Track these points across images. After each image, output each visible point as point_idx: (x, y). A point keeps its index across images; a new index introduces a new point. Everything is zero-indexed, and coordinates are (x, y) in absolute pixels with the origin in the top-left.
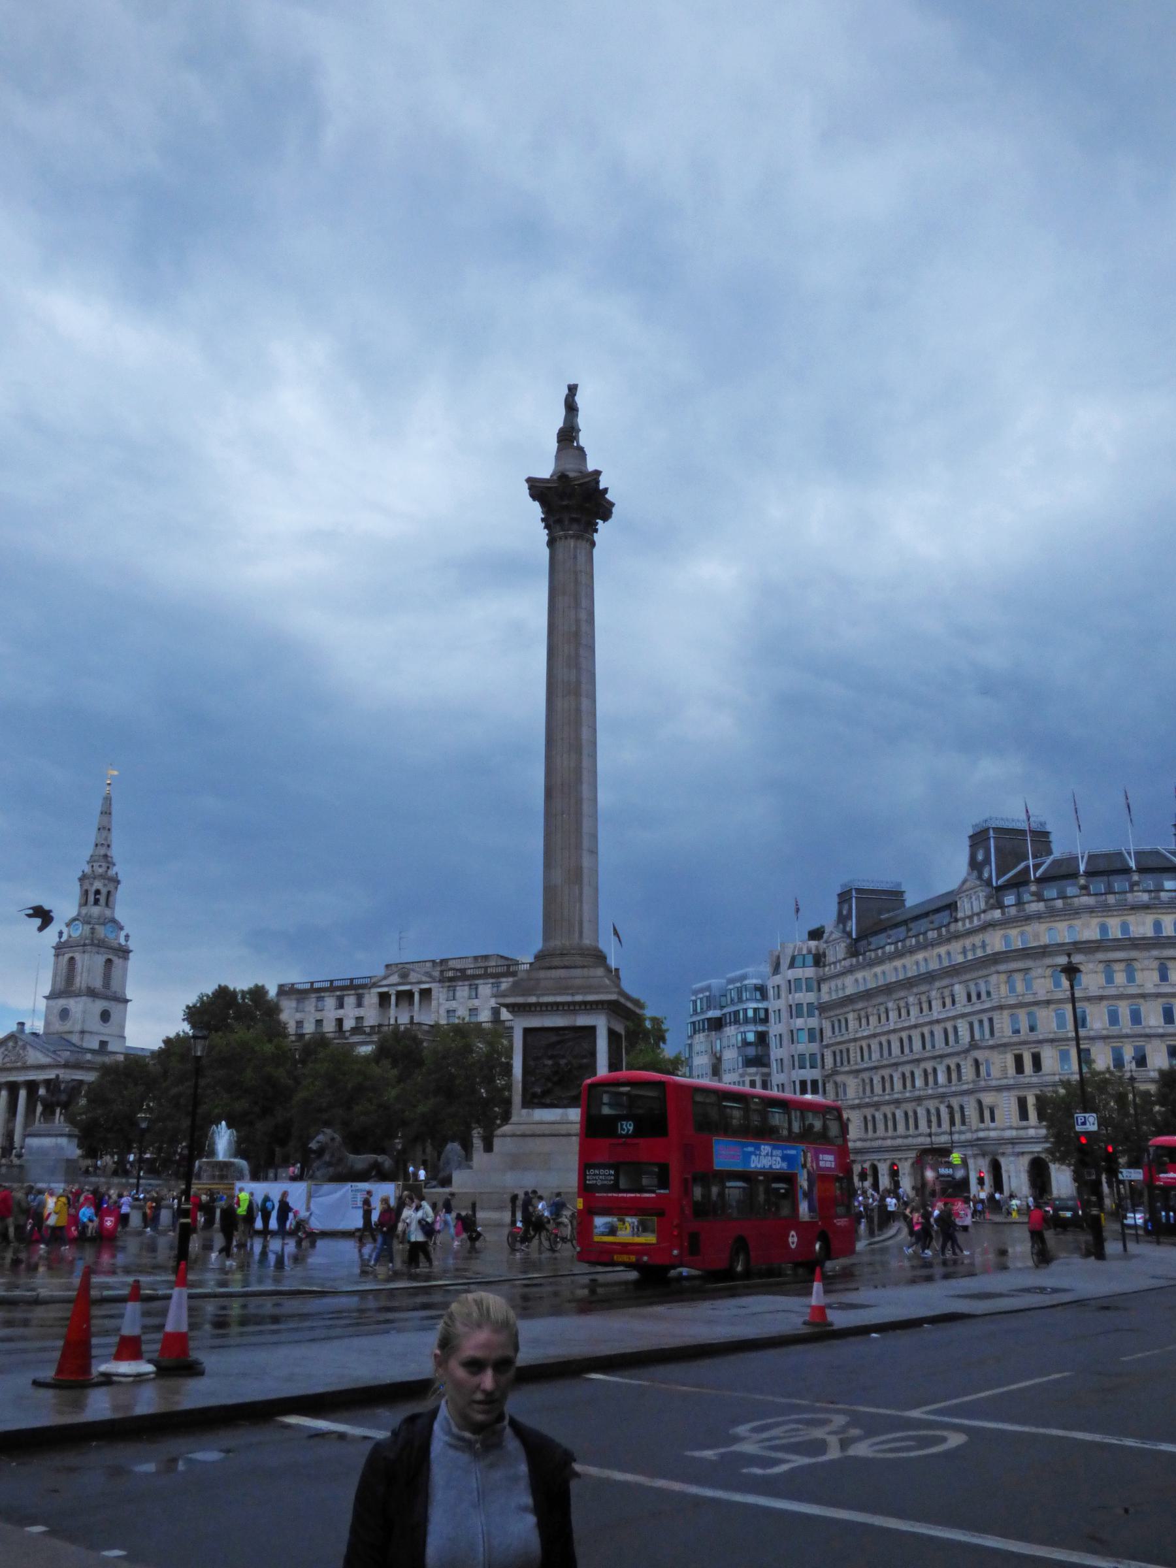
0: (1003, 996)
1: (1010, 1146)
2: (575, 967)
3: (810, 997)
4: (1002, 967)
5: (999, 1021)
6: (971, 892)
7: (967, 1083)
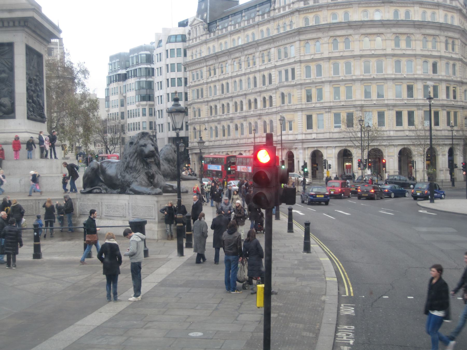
0: (301, 55)
1: (301, 144)
3: (180, 60)
4: (303, 37)
5: (299, 70)
7: (276, 108)
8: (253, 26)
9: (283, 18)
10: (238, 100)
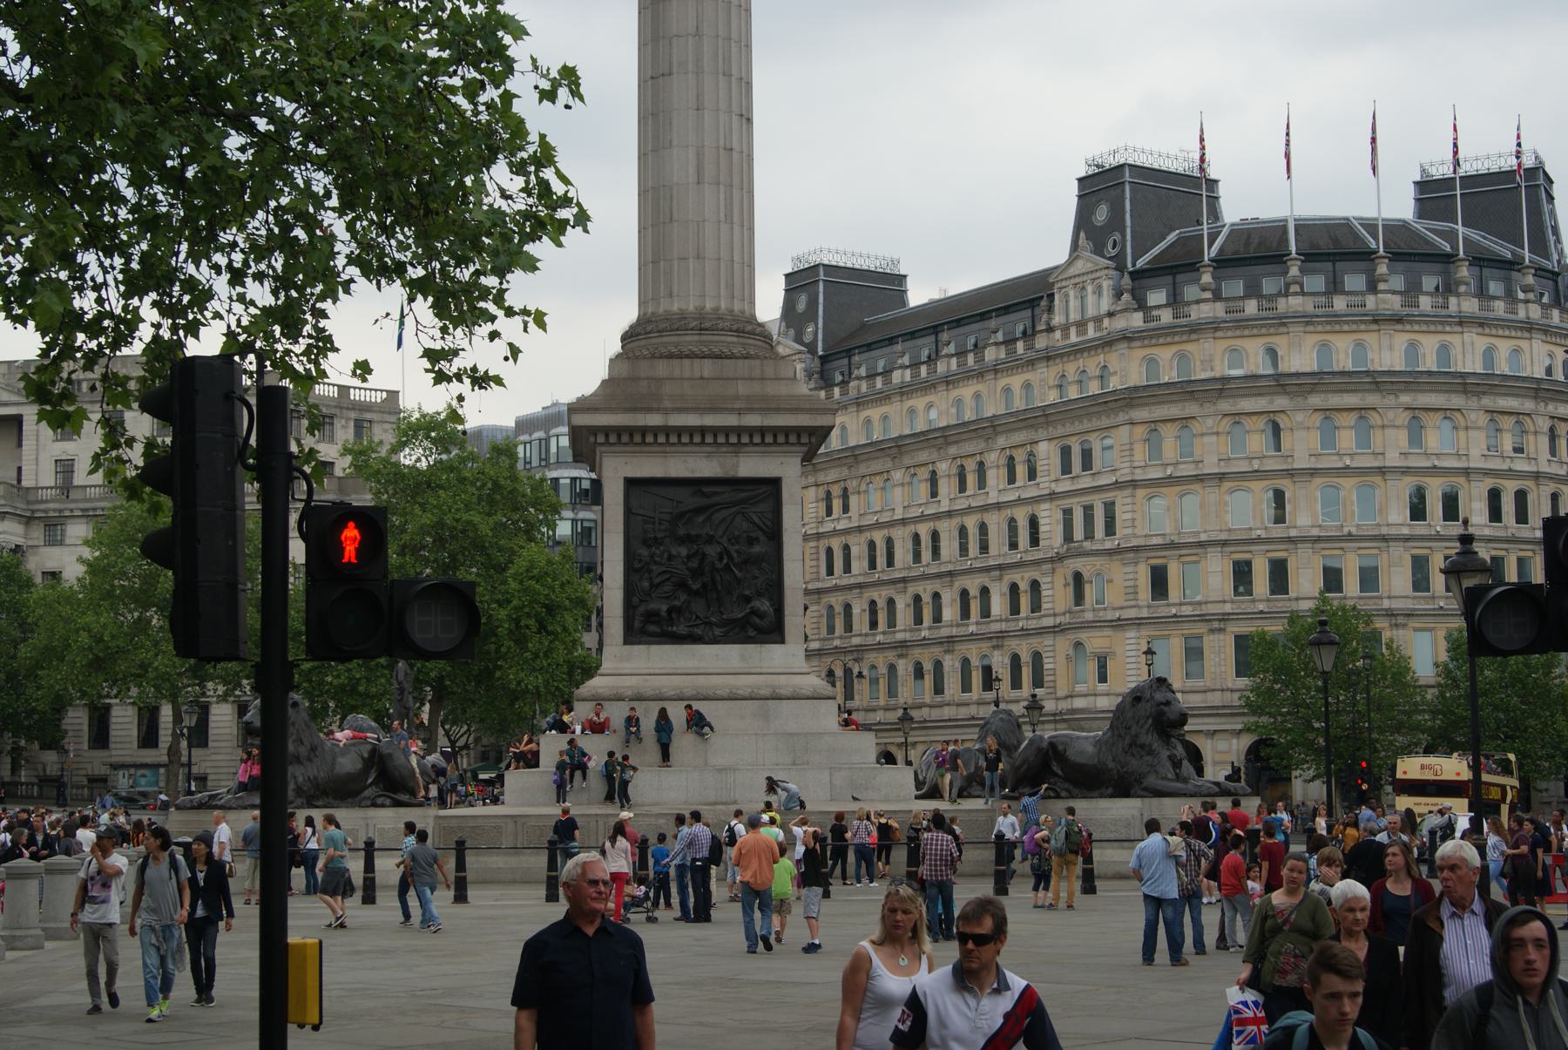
0: (1136, 464)
2: (732, 357)
4: (1141, 414)
5: (1129, 508)
6: (1085, 278)
7: (1055, 615)
8: (980, 375)
9: (1078, 356)
10: (925, 590)
